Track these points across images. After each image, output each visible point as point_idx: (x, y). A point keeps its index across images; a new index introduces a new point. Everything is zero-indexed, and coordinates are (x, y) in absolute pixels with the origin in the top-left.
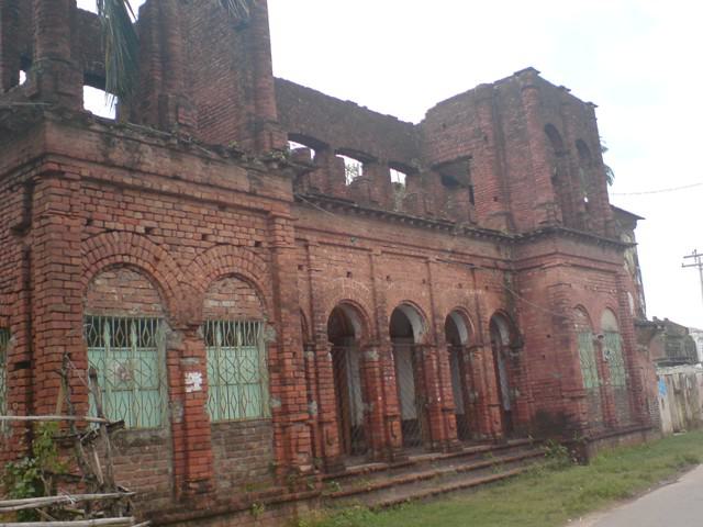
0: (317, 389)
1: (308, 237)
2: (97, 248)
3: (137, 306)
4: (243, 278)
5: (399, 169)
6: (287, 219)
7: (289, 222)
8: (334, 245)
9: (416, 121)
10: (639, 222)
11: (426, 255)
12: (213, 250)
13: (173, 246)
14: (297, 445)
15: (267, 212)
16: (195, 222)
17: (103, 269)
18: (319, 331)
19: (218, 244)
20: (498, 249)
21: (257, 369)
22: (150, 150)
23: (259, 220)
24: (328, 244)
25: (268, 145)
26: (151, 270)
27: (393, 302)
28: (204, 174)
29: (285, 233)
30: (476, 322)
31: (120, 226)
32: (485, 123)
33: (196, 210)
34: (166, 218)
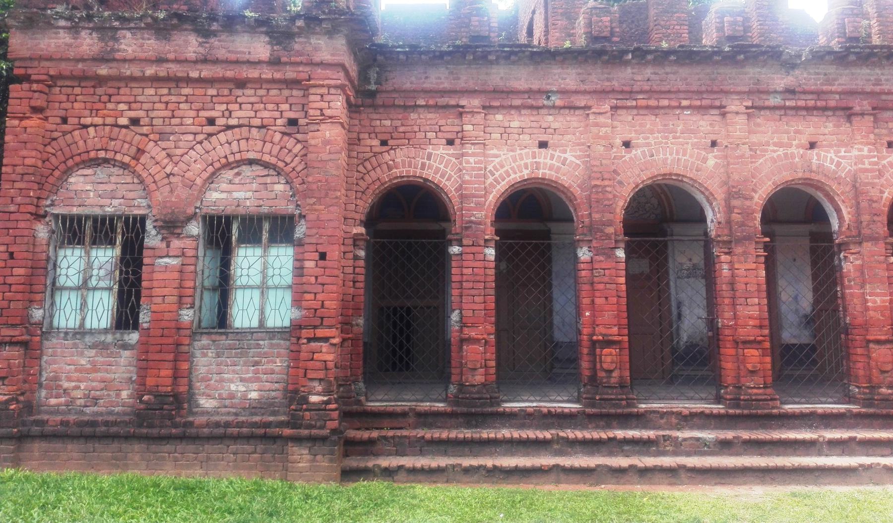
1: (463, 102)
8: (512, 107)
11: (717, 103)
18: (471, 222)
19: (229, 127)
22: (128, 34)
24: (502, 107)
28: (201, 50)
29: (324, 105)
31: (98, 120)
34: (157, 106)
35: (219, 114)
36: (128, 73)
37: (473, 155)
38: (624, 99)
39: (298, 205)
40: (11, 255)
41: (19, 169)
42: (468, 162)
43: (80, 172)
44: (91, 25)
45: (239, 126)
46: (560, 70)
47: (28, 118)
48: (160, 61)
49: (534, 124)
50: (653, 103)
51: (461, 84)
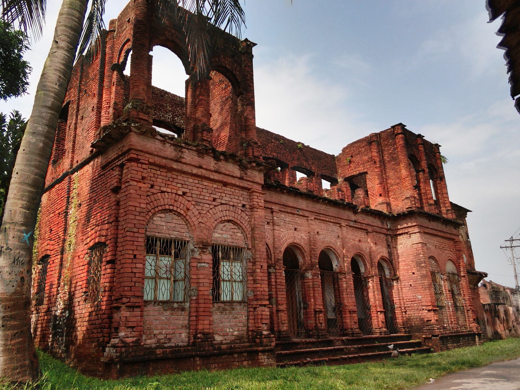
0: (276, 291)
1: (273, 207)
2: (156, 200)
3: (176, 233)
4: (235, 223)
5: (327, 179)
6: (260, 193)
7: (261, 195)
9: (336, 154)
10: (468, 213)
12: (219, 207)
13: (197, 203)
14: (262, 319)
15: (249, 189)
16: (210, 192)
17: (158, 211)
19: (222, 204)
20: (383, 223)
21: (241, 274)
22: (187, 151)
23: (244, 193)
24: (284, 212)
25: (251, 154)
26: (185, 215)
27: (320, 247)
30: (370, 262)
31: (169, 190)
32: (375, 154)
33: (211, 185)
34: (194, 188)
35: (218, 197)
36: (186, 170)
37: (278, 230)
38: (319, 217)
39: (246, 244)
40: (135, 256)
41: (138, 209)
42: (276, 233)
43: (159, 215)
44: (172, 142)
45: (226, 204)
46: (300, 201)
47: (140, 182)
48: (200, 167)
49: (293, 221)
50: (324, 219)
51: (273, 200)
